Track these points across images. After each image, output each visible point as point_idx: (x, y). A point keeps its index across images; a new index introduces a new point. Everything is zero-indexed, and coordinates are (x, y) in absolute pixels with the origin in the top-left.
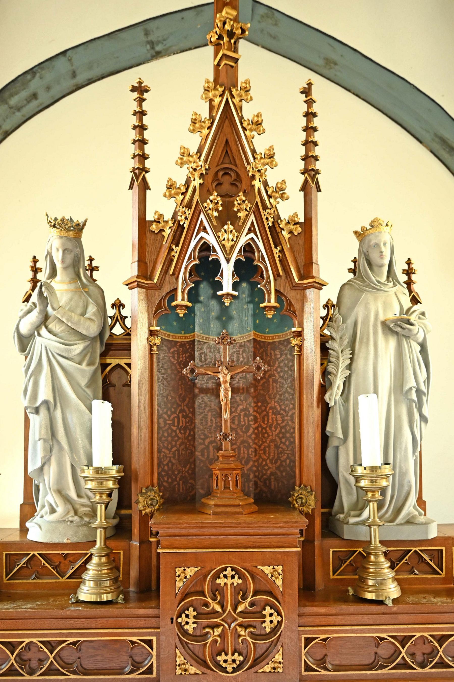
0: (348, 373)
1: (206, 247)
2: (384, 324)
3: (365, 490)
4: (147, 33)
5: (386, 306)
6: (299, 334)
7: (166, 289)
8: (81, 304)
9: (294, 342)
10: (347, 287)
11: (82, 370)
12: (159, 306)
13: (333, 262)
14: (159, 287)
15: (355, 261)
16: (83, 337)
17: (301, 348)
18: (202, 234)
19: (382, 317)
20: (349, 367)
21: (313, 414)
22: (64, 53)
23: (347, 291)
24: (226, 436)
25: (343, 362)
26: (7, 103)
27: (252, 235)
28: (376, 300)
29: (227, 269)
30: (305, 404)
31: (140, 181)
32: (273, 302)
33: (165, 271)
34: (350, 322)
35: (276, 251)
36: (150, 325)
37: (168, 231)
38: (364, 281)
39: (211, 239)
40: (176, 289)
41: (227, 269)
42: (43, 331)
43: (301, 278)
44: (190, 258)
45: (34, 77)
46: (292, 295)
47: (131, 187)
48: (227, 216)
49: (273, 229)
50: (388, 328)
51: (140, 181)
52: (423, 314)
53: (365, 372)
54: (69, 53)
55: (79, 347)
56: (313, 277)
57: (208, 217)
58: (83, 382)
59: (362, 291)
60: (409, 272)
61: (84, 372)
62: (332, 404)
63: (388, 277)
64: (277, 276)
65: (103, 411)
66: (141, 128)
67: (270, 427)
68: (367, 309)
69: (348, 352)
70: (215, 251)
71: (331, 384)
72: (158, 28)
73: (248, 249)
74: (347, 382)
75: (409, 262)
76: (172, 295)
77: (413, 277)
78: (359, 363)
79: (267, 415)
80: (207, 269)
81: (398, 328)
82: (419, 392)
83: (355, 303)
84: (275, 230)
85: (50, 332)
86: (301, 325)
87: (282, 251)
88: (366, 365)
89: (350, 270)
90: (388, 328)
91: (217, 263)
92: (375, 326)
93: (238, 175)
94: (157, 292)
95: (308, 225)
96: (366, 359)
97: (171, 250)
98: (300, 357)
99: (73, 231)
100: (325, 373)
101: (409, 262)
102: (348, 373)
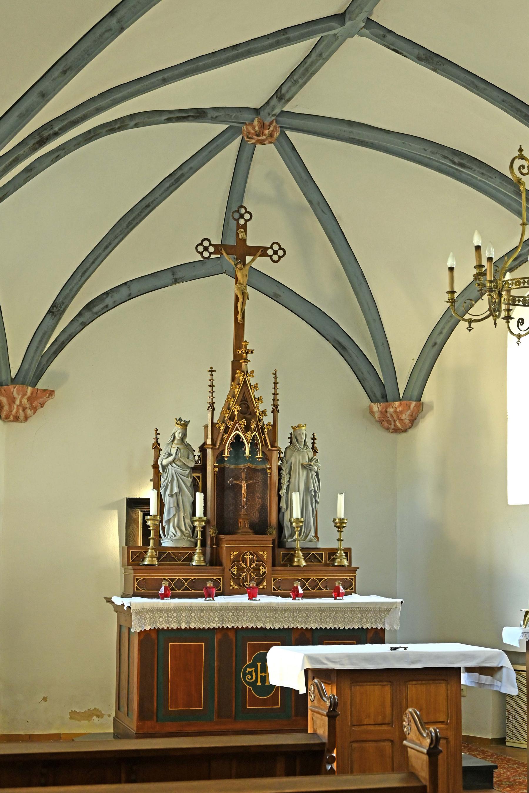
0: (288, 483)
2: (302, 465)
3: (294, 527)
4: (173, 274)
5: (303, 457)
6: (270, 468)
7: (221, 449)
8: (187, 454)
9: (268, 471)
10: (288, 449)
11: (188, 481)
12: (217, 457)
14: (219, 449)
15: (291, 434)
16: (188, 467)
17: (271, 473)
18: (237, 432)
19: (301, 462)
20: (289, 481)
21: (275, 499)
22: (126, 283)
23: (288, 450)
24: (244, 507)
25: (286, 479)
26: (91, 311)
27: (255, 432)
28: (299, 454)
30: (272, 496)
31: (212, 407)
32: (261, 456)
33: (221, 443)
34: (289, 463)
35: (263, 437)
36: (214, 463)
37: (222, 428)
38: (294, 447)
39: (241, 434)
40: (224, 450)
42: (174, 465)
43: (272, 446)
44: (231, 439)
45: (107, 296)
46: (268, 453)
47: (208, 410)
49: (262, 428)
50: (304, 467)
52: (317, 460)
53: (295, 483)
54: (128, 284)
55: (188, 472)
56: (276, 447)
57: (241, 427)
58: (189, 485)
59: (294, 451)
60: (313, 439)
62: (282, 495)
63: (304, 444)
64: (262, 445)
65: (200, 496)
66: (212, 386)
67: (256, 504)
68: (296, 458)
69: (288, 475)
70: (242, 439)
71: (282, 487)
72: (180, 271)
73: (255, 436)
74: (288, 487)
75: (313, 434)
76: (223, 452)
77: (315, 441)
78: (292, 480)
79: (255, 499)
80: (237, 443)
81: (307, 467)
82: (315, 491)
83: (291, 456)
85: (176, 465)
86: (271, 465)
87: (265, 436)
88: (295, 481)
89: (289, 438)
90: (304, 467)
91: (243, 443)
92: (299, 465)
93: (248, 405)
94: (217, 450)
95: (274, 425)
96: (295, 478)
97: (223, 435)
98: (270, 477)
99: (185, 425)
100: (280, 483)
101: (313, 434)
102: (288, 483)
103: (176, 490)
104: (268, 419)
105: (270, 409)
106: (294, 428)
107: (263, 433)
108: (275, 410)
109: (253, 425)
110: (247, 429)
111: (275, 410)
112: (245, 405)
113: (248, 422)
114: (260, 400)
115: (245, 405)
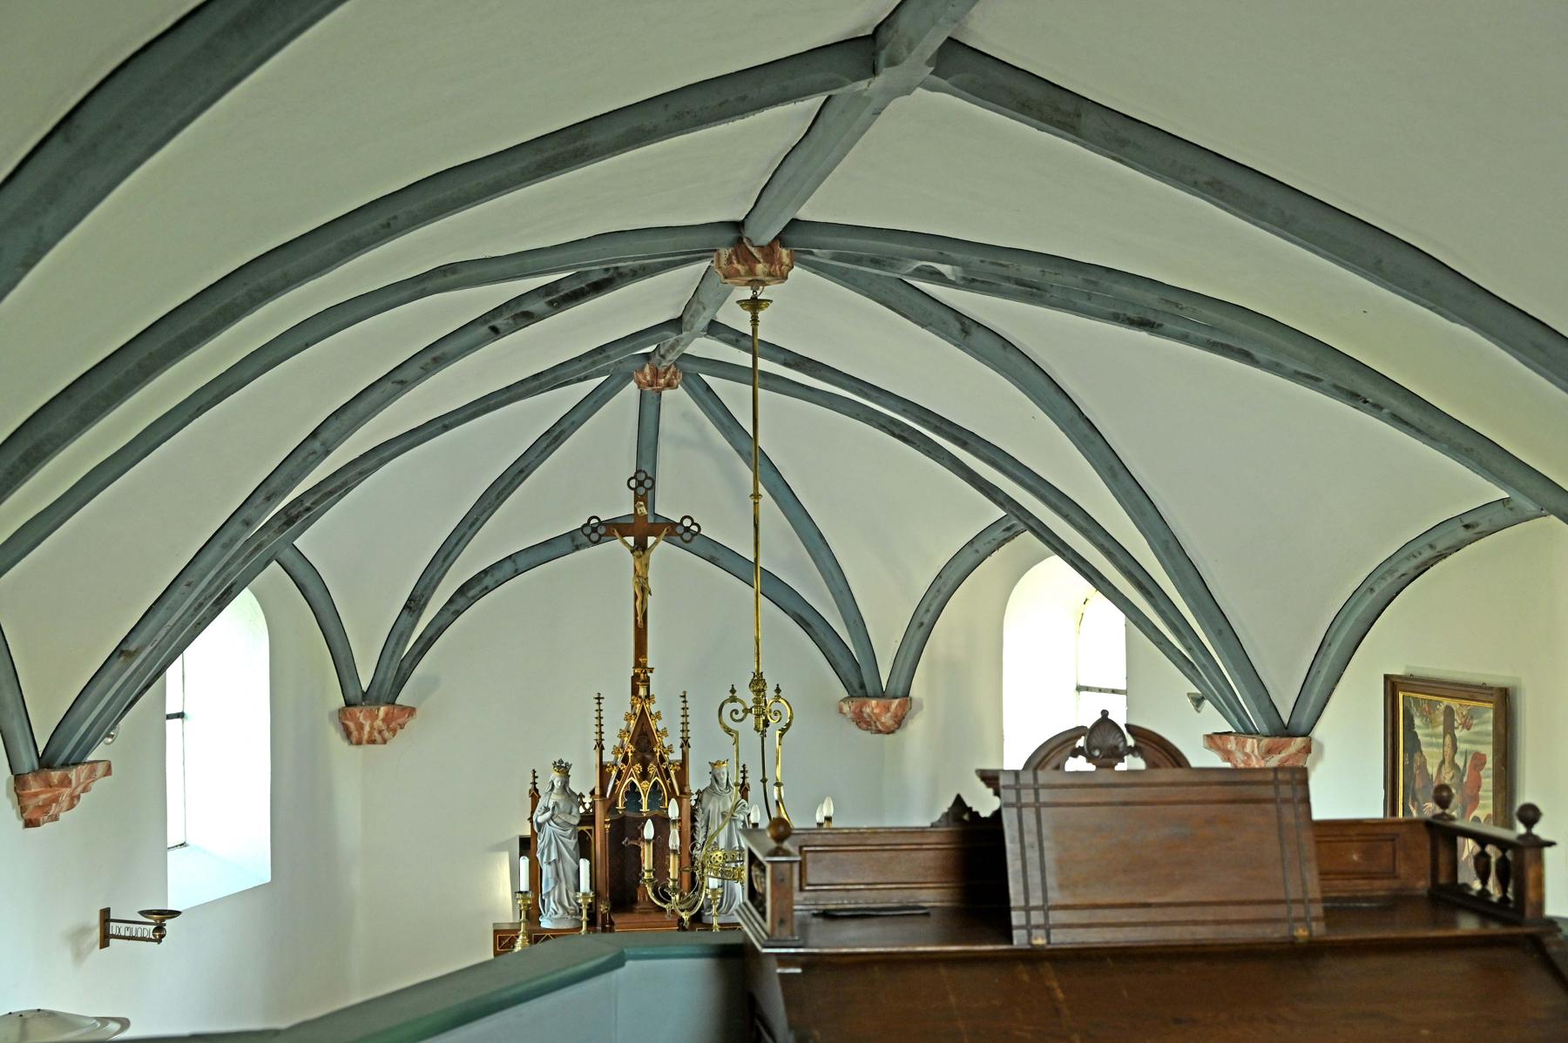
1: (633, 784)
5: (725, 804)
13: (697, 781)
29: (644, 801)
31: (600, 747)
41: (644, 801)
48: (644, 776)
51: (600, 747)
61: (572, 843)
65: (584, 865)
73: (656, 783)
76: (616, 804)
80: (633, 793)
84: (667, 771)
95: (684, 763)
99: (563, 769)
103: (554, 856)
104: (676, 756)
105: (680, 741)
106: (713, 765)
107: (668, 776)
108: (685, 743)
109: (652, 769)
110: (644, 776)
111: (685, 743)
112: (643, 738)
113: (645, 765)
114: (664, 733)
115: (643, 738)
